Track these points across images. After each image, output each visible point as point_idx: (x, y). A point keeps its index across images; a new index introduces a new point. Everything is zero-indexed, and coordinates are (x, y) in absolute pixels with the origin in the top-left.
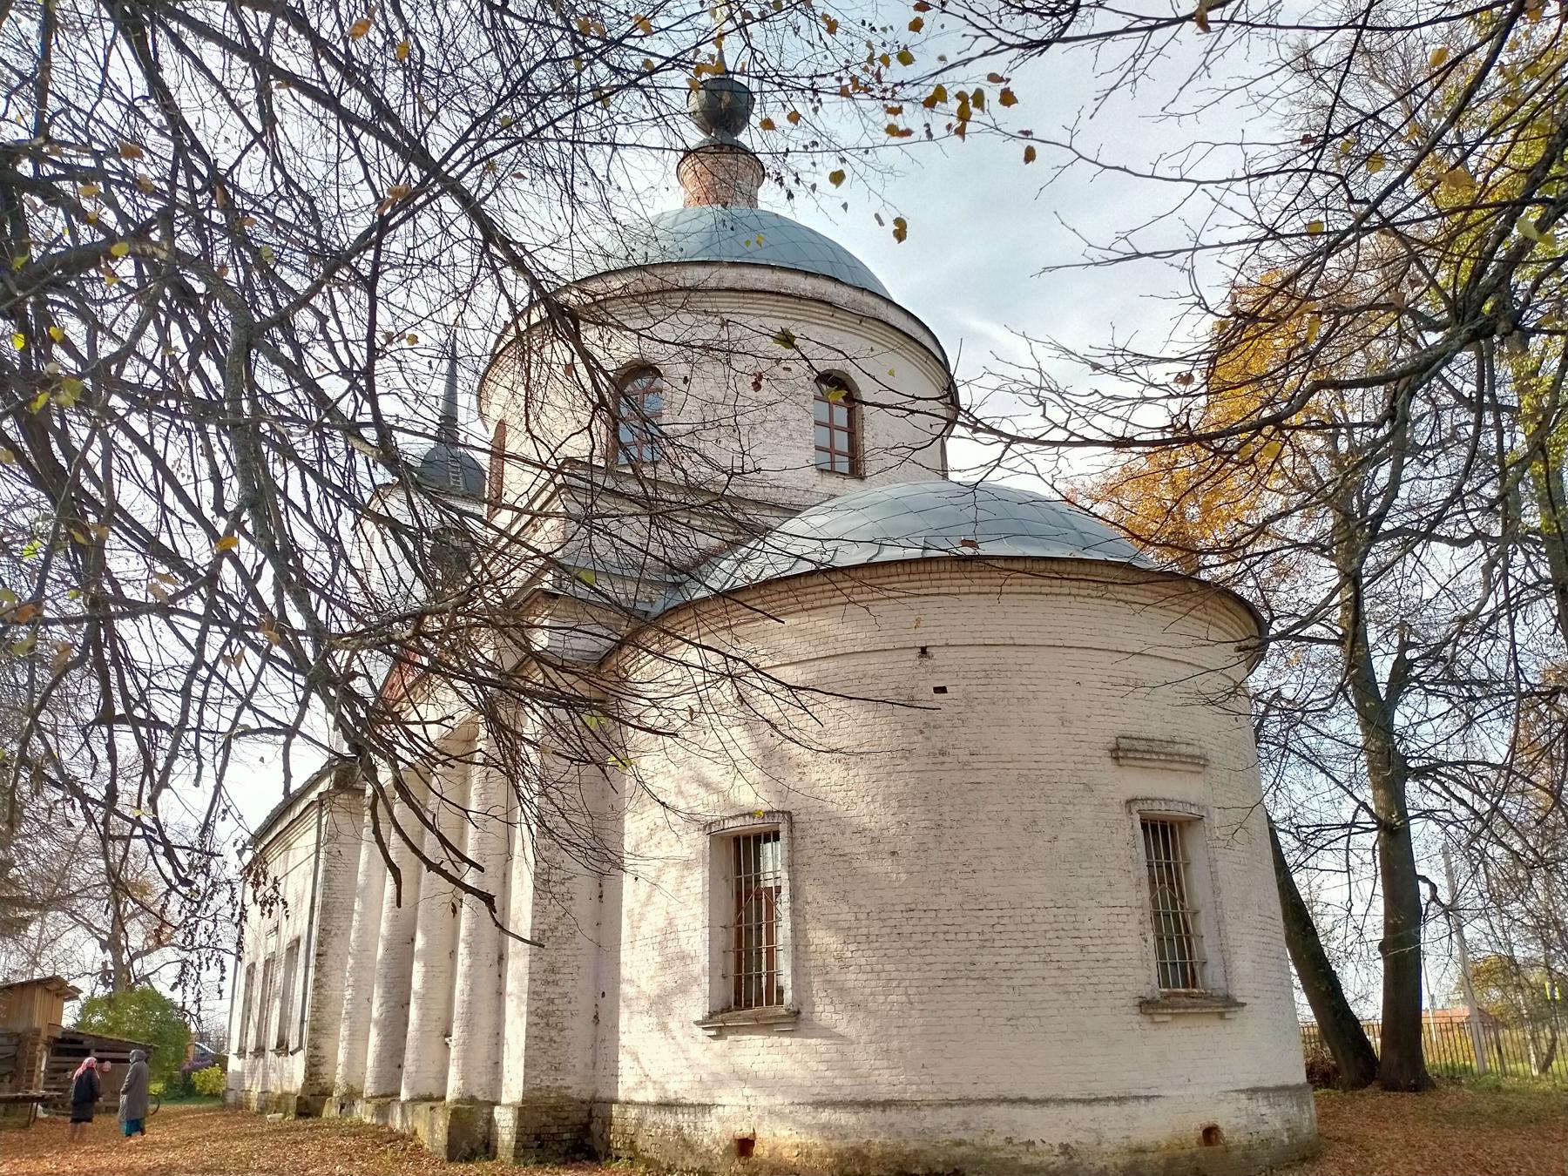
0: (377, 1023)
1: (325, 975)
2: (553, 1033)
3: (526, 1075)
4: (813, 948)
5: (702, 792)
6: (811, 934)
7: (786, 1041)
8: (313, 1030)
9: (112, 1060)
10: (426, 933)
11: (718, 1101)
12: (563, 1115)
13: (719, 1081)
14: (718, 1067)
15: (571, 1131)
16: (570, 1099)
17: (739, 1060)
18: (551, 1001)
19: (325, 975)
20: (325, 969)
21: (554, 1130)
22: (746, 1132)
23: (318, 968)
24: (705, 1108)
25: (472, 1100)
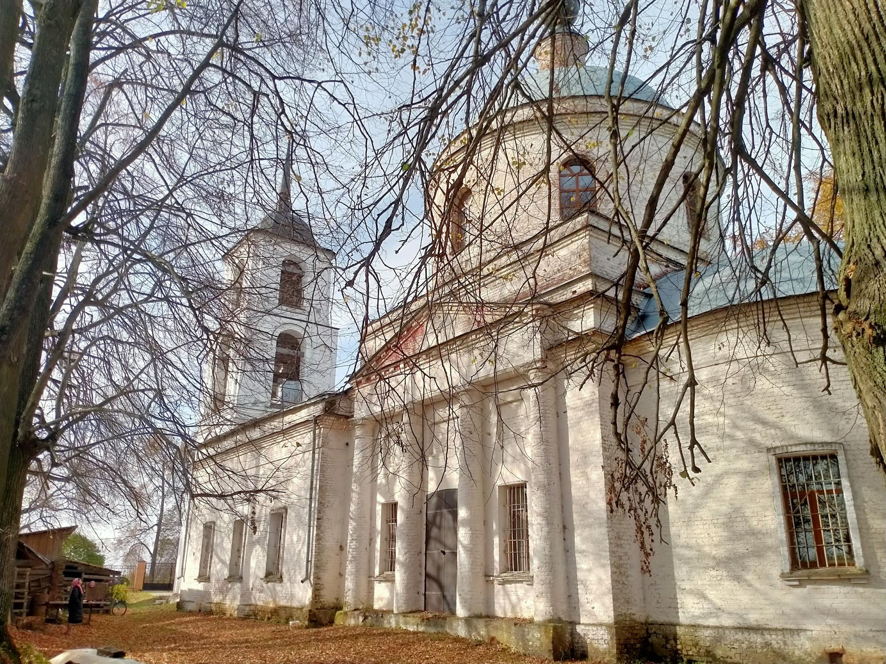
0: (402, 564)
1: (322, 532)
2: (624, 578)
3: (614, 606)
4: (873, 531)
5: (759, 427)
6: (871, 522)
7: (861, 590)
8: (317, 567)
9: (96, 580)
10: (469, 507)
11: (804, 627)
12: (635, 632)
13: (805, 615)
14: (802, 606)
15: (639, 643)
16: (636, 622)
17: (820, 601)
18: (620, 558)
19: (322, 532)
20: (323, 528)
21: (632, 642)
22: (834, 647)
23: (319, 527)
24: (799, 631)
25: (560, 620)
